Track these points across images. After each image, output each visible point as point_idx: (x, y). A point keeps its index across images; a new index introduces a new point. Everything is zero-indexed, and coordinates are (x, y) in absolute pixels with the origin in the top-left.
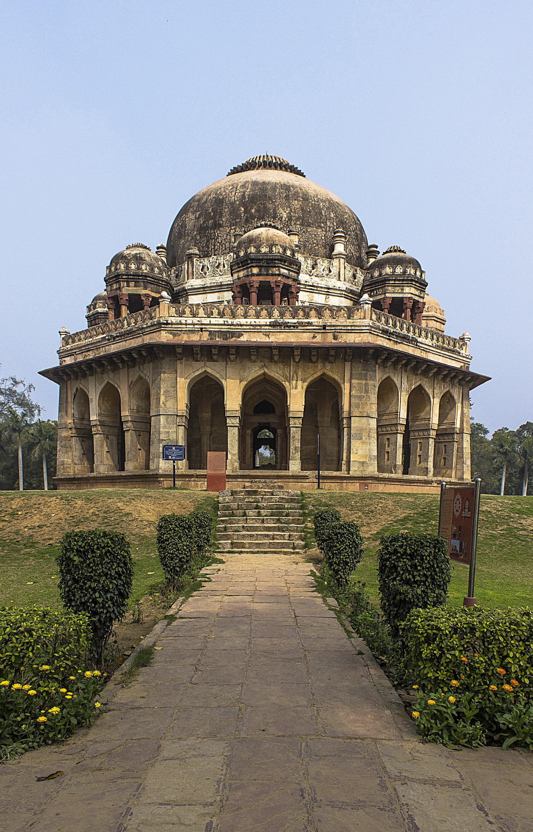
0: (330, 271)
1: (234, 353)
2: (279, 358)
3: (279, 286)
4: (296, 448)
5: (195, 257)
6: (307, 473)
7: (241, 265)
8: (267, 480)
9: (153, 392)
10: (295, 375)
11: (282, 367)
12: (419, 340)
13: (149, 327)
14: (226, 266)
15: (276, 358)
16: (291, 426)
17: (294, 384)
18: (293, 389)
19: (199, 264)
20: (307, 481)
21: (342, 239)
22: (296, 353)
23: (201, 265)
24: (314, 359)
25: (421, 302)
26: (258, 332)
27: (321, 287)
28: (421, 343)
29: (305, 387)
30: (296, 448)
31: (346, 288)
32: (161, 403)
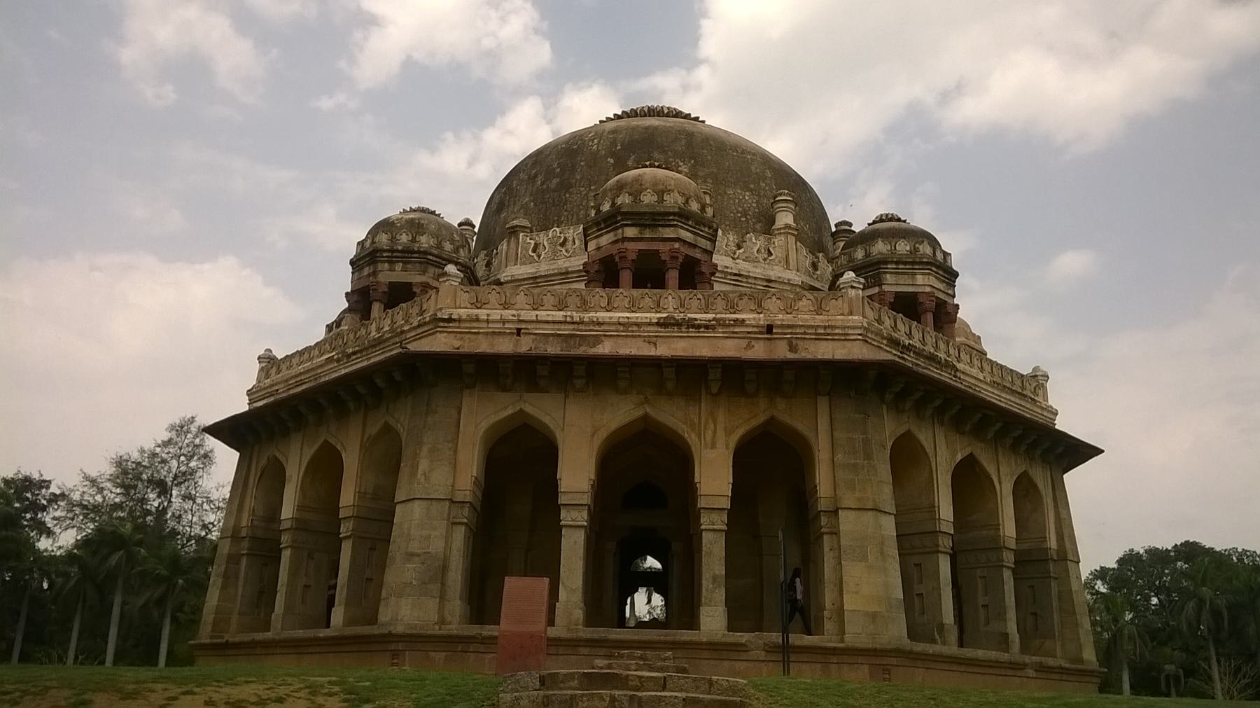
0: (770, 254)
3: (677, 258)
4: (715, 578)
5: (523, 232)
6: (742, 637)
7: (603, 226)
8: (649, 653)
9: (406, 453)
10: (710, 421)
12: (960, 366)
13: (415, 328)
14: (577, 241)
15: (670, 385)
16: (703, 527)
17: (709, 438)
18: (706, 448)
19: (528, 241)
20: (745, 656)
21: (790, 205)
22: (711, 376)
23: (533, 242)
25: (949, 304)
26: (633, 336)
27: (755, 278)
28: (963, 373)
29: (732, 445)
30: (715, 578)
31: (802, 282)
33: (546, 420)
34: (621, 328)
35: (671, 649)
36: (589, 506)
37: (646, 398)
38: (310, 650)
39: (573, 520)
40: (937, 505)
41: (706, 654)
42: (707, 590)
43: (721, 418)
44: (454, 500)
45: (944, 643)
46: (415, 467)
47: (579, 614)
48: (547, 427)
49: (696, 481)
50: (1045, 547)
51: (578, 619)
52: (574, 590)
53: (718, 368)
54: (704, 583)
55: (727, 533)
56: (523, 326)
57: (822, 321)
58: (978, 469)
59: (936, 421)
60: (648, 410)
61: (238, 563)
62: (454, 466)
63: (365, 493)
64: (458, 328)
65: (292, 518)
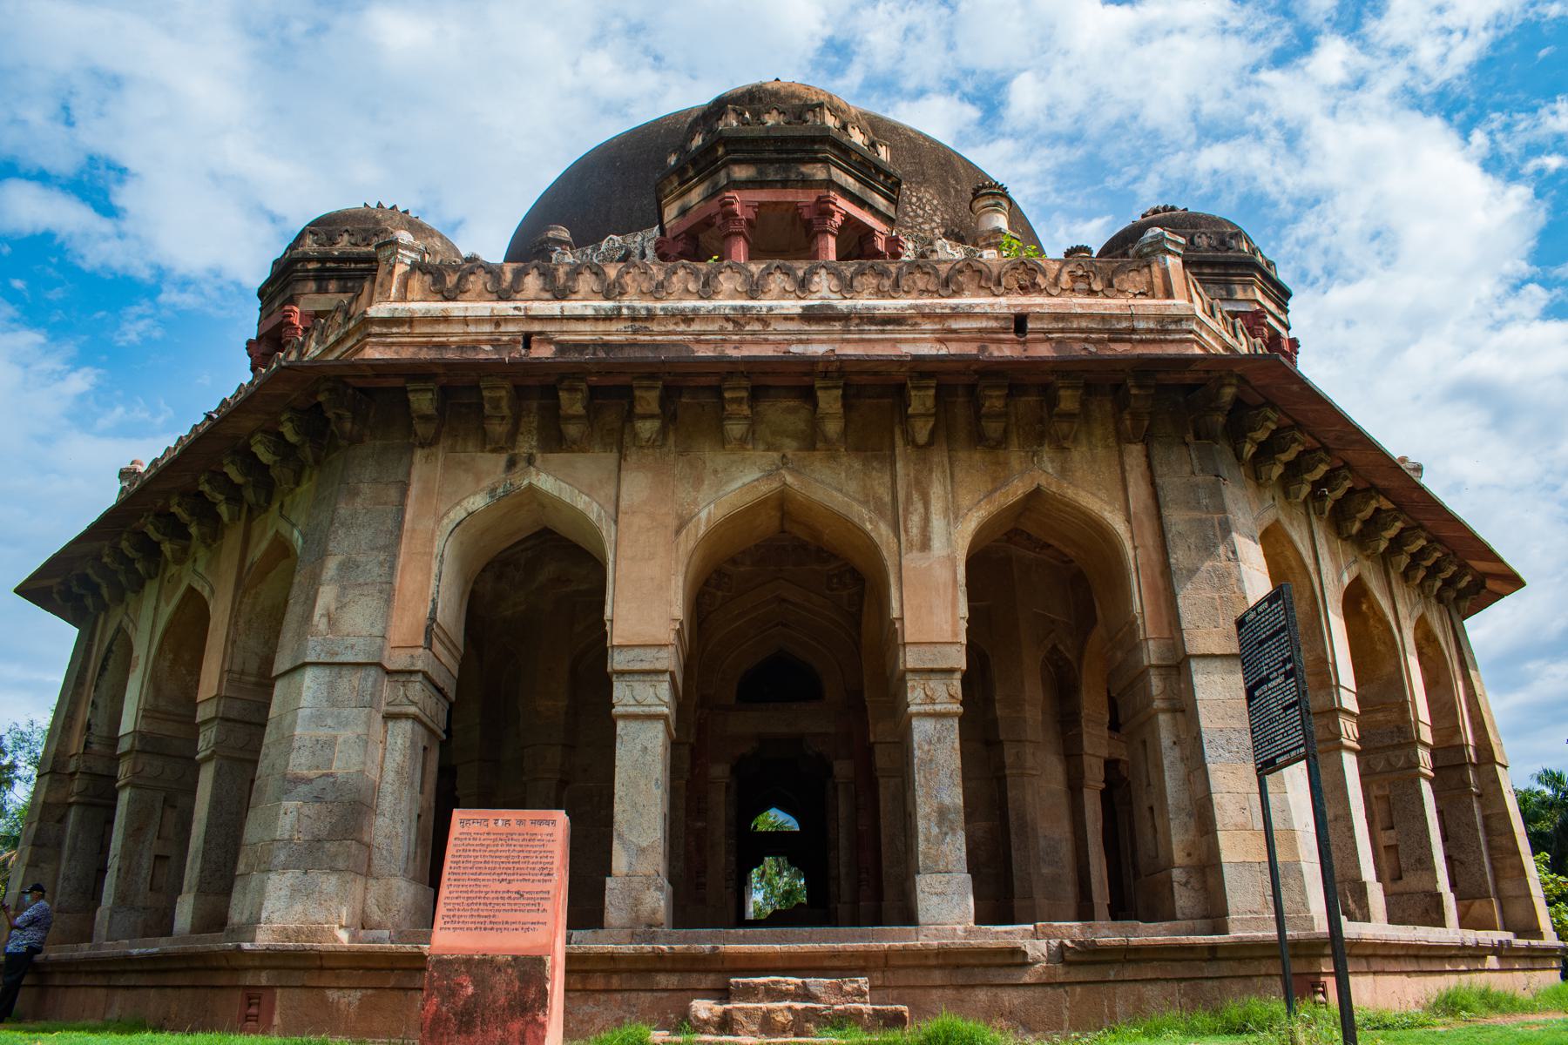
1: (657, 410)
2: (845, 432)
4: (942, 813)
8: (816, 983)
10: (916, 497)
11: (857, 465)
16: (913, 709)
17: (915, 531)
18: (911, 548)
24: (993, 428)
30: (942, 813)
32: (318, 611)
33: (581, 502)
34: (730, 327)
35: (862, 971)
36: (672, 674)
37: (784, 456)
38: (122, 981)
39: (639, 704)
40: (1330, 660)
41: (937, 977)
42: (928, 840)
43: (937, 491)
44: (390, 666)
45: (1366, 918)
46: (311, 601)
47: (657, 901)
48: (582, 516)
49: (895, 614)
50: (1458, 742)
51: (654, 912)
52: (643, 850)
53: (928, 387)
54: (921, 825)
55: (963, 720)
56: (536, 327)
57: (1120, 307)
58: (1364, 607)
59: (1312, 512)
60: (789, 479)
61: (62, 820)
62: (388, 595)
63: (242, 673)
64: (407, 335)
65: (134, 731)
